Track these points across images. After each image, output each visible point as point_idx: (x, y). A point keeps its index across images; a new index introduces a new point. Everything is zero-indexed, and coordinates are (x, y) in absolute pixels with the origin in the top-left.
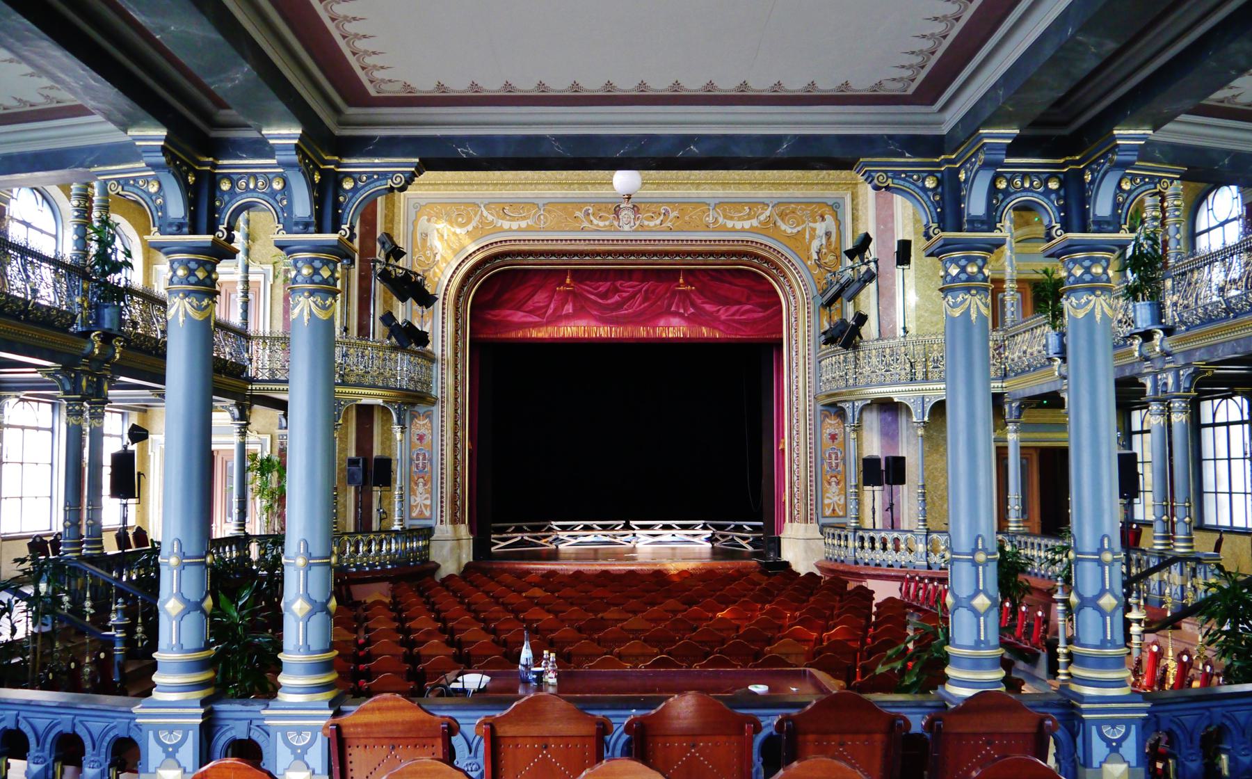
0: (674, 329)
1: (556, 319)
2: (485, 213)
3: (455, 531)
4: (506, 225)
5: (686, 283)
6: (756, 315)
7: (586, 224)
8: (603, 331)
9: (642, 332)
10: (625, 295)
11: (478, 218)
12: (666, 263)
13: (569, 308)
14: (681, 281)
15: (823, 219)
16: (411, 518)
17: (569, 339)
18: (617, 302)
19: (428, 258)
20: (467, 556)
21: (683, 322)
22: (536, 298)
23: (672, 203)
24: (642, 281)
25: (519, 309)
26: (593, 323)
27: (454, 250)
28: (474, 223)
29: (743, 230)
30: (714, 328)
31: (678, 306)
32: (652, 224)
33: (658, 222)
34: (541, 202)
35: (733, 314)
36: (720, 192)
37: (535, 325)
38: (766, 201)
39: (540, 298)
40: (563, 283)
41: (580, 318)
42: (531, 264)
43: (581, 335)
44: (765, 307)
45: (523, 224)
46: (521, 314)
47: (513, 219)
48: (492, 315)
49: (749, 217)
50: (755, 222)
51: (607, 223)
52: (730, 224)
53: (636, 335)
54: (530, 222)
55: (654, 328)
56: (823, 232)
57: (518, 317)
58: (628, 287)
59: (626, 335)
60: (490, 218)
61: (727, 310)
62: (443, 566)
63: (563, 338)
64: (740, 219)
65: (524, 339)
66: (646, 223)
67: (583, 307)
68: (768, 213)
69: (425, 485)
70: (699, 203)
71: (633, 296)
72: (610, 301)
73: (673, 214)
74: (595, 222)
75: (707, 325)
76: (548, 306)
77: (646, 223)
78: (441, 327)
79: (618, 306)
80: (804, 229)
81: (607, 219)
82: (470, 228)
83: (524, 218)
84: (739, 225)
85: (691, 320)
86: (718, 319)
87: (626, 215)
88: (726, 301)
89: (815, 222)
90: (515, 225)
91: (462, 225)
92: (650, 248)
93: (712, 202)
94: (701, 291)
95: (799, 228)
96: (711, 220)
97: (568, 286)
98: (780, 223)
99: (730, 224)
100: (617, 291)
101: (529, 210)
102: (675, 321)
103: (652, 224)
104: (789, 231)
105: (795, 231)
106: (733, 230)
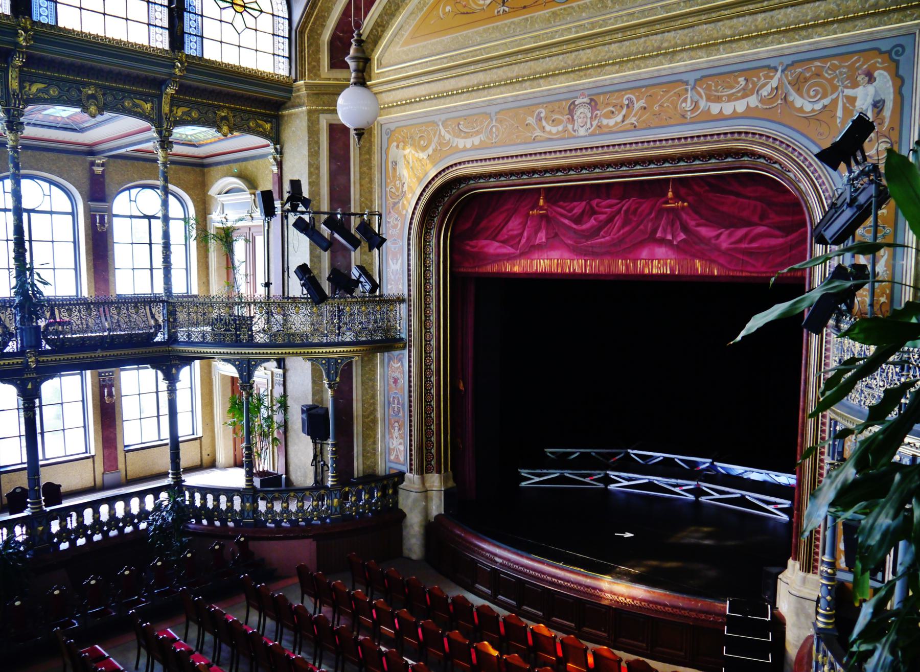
0: (658, 263)
1: (531, 250)
3: (423, 482)
4: (461, 143)
5: (677, 197)
6: (773, 242)
7: (538, 133)
8: (577, 265)
9: (620, 267)
10: (602, 217)
11: (436, 140)
12: (639, 175)
13: (542, 237)
14: (670, 194)
15: (871, 79)
16: (390, 461)
17: (542, 274)
18: (592, 227)
19: (397, 189)
20: (436, 507)
21: (670, 253)
22: (511, 225)
23: (636, 87)
24: (622, 198)
25: (494, 239)
26: (566, 255)
27: (418, 178)
28: (433, 146)
29: (735, 116)
30: (712, 261)
31: (665, 231)
32: (611, 122)
33: (619, 118)
34: (493, 110)
35: (740, 241)
36: (702, 60)
37: (510, 258)
38: (772, 63)
39: (514, 225)
40: (535, 206)
42: (491, 186)
43: (554, 270)
44: (786, 230)
45: (476, 140)
46: (497, 244)
47: (467, 135)
51: (560, 128)
52: (715, 108)
53: (614, 270)
55: (635, 261)
56: (870, 101)
57: (493, 248)
58: (606, 206)
59: (603, 270)
61: (730, 235)
62: (408, 516)
63: (536, 273)
64: (730, 98)
66: (605, 122)
67: (556, 235)
68: (774, 83)
69: (399, 430)
70: (674, 82)
71: (610, 220)
72: (584, 227)
73: (638, 105)
77: (605, 122)
78: (396, 268)
79: (595, 232)
80: (835, 102)
82: (430, 151)
83: (477, 133)
84: (728, 108)
85: (682, 250)
86: (717, 248)
87: (583, 113)
88: (732, 222)
89: (855, 85)
90: (468, 143)
91: (424, 149)
92: (607, 157)
93: (691, 78)
94: (694, 209)
95: (826, 101)
96: (688, 106)
97: (541, 208)
98: (794, 97)
99: (715, 108)
100: (593, 212)
102: (661, 251)
103: (611, 122)
104: (808, 107)
105: (818, 106)
106: (721, 117)
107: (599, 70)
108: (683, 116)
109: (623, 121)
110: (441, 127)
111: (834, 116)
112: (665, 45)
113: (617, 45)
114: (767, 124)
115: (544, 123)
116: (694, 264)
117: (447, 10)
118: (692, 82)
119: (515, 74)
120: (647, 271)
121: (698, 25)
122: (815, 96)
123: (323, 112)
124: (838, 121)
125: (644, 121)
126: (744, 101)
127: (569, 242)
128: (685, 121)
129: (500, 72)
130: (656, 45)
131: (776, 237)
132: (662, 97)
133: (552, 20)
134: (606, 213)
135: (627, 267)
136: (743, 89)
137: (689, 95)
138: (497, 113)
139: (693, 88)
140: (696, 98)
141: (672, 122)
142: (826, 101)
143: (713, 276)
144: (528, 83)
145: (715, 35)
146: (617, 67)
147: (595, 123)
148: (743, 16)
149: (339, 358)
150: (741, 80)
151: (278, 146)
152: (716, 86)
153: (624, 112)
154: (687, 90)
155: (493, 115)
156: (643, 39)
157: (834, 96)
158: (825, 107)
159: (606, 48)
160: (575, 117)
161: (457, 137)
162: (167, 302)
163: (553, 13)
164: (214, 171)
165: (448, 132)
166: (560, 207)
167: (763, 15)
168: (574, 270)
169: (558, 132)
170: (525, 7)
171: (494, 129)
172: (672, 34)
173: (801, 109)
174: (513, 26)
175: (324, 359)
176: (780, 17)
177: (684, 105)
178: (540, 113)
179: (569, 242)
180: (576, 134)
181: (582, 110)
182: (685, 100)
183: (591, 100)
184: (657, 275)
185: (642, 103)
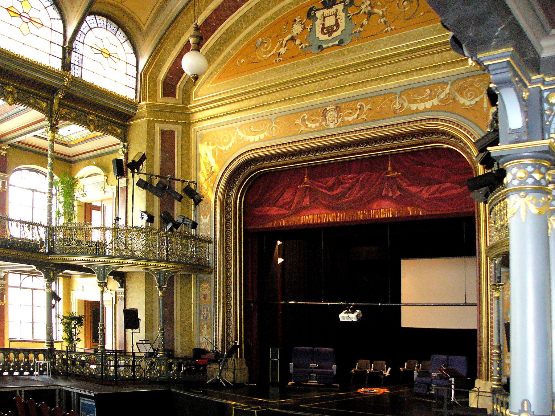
2: (239, 133)
7: (303, 128)
23: (365, 98)
29: (426, 110)
30: (418, 207)
32: (350, 119)
33: (355, 116)
36: (404, 80)
38: (445, 80)
41: (314, 208)
45: (262, 136)
47: (256, 134)
48: (258, 211)
49: (431, 98)
50: (435, 101)
51: (318, 124)
52: (414, 107)
54: (266, 134)
60: (242, 135)
64: (422, 101)
65: (278, 227)
66: (346, 119)
68: (447, 91)
70: (388, 94)
74: (309, 125)
75: (412, 205)
76: (293, 200)
77: (346, 119)
81: (317, 121)
83: (263, 132)
84: (421, 106)
93: (398, 91)
95: (477, 99)
96: (397, 106)
99: (414, 107)
101: (266, 125)
103: (350, 119)
104: (467, 103)
105: (473, 102)
106: (417, 112)
107: (341, 90)
108: (395, 113)
109: (358, 118)
110: (238, 130)
111: (482, 107)
112: (381, 73)
113: (351, 75)
114: (445, 114)
115: (307, 122)
116: (407, 209)
117: (242, 61)
118: (399, 93)
119: (287, 95)
120: (377, 217)
121: (400, 61)
122: (471, 97)
123: (158, 122)
124: (485, 109)
125: (371, 117)
126: (430, 102)
127: (325, 203)
128: (395, 115)
129: (277, 95)
130: (375, 74)
131: (456, 189)
132: (382, 102)
133: (310, 63)
134: (349, 183)
135: (364, 215)
136: (430, 95)
137: (397, 100)
138: (275, 119)
139: (400, 97)
140: (402, 102)
141: (388, 116)
142: (477, 99)
143: (418, 216)
144: (295, 100)
145: (411, 67)
146: (352, 87)
147: (340, 120)
148: (426, 55)
149: (167, 271)
150: (428, 90)
151: (126, 144)
152: (413, 95)
153: (358, 112)
154: (396, 98)
155: (273, 119)
156: (367, 71)
157: (482, 96)
158: (477, 102)
159: (345, 77)
160: (327, 118)
161: (249, 135)
162: (49, 227)
163: (311, 59)
164: (78, 165)
165: (243, 133)
166: (318, 181)
167: (437, 55)
168: (329, 220)
169: (316, 127)
170: (293, 57)
171: (274, 129)
172: (385, 67)
173: (464, 104)
174: (285, 68)
175: (156, 270)
176: (447, 56)
177: (395, 106)
178: (304, 117)
179: (325, 203)
180: (328, 127)
181: (331, 113)
182: (395, 103)
183: (337, 107)
184: (383, 218)
185: (369, 107)
